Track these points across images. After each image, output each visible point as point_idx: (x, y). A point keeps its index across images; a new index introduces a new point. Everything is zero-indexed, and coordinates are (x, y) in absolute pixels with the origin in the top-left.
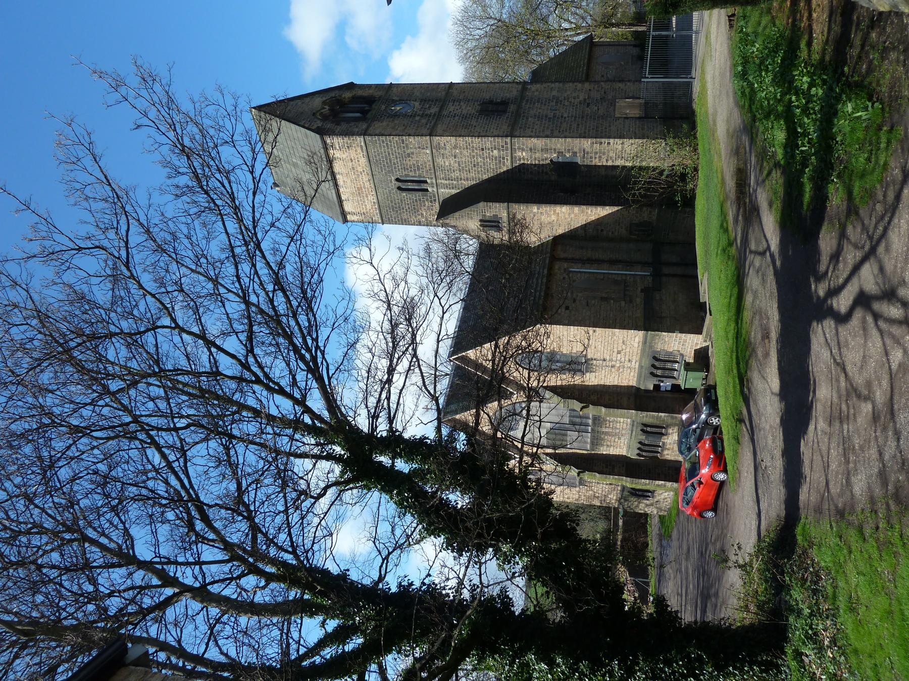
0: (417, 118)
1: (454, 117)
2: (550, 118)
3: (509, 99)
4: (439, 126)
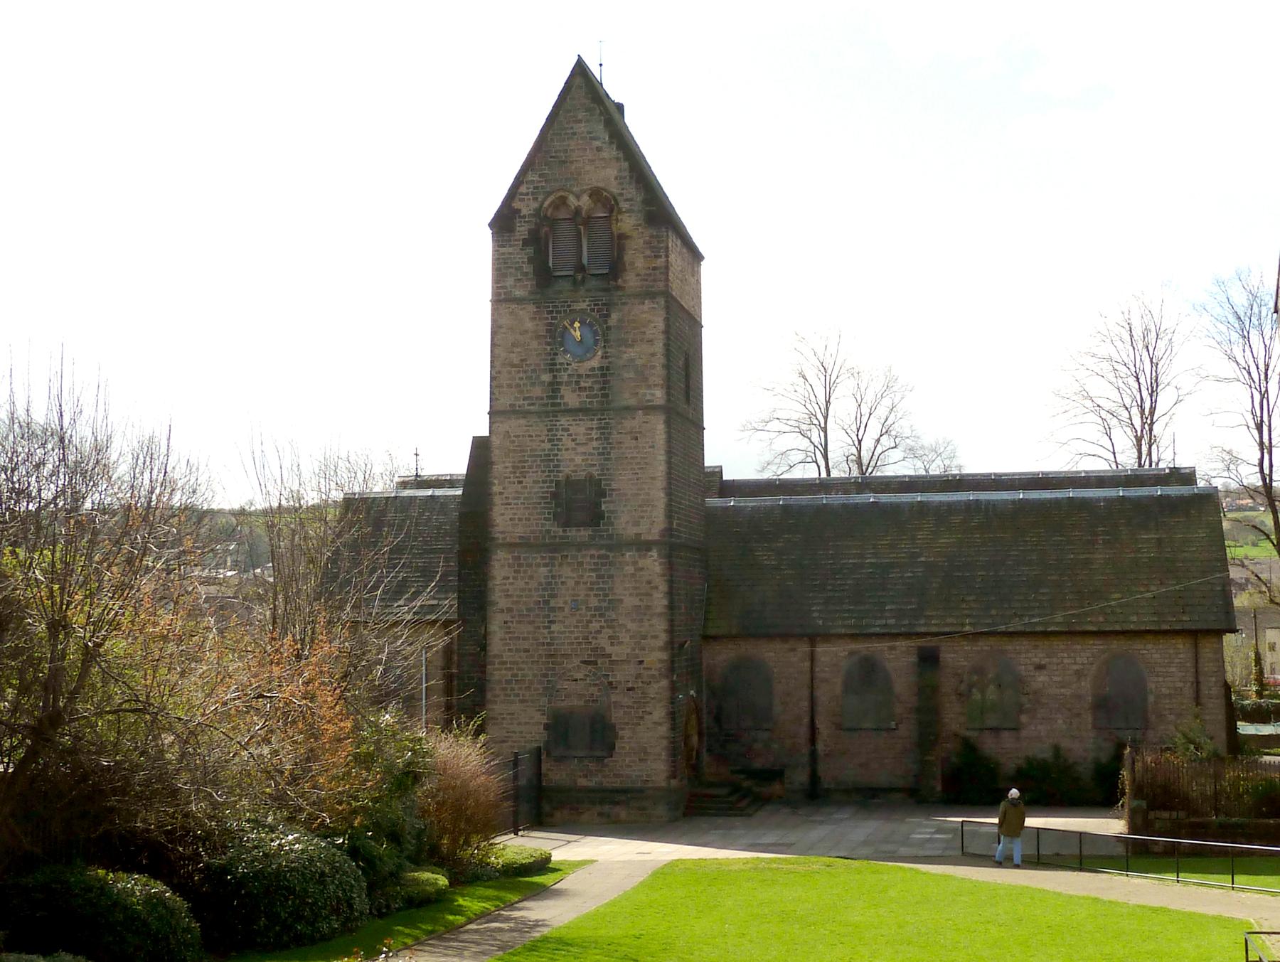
0: (546, 378)
1: (550, 441)
2: (547, 602)
3: (612, 524)
4: (522, 422)
